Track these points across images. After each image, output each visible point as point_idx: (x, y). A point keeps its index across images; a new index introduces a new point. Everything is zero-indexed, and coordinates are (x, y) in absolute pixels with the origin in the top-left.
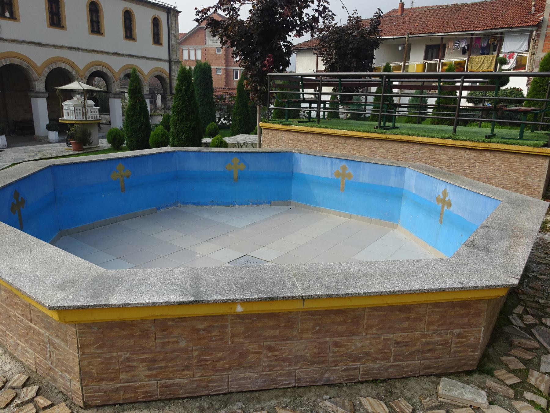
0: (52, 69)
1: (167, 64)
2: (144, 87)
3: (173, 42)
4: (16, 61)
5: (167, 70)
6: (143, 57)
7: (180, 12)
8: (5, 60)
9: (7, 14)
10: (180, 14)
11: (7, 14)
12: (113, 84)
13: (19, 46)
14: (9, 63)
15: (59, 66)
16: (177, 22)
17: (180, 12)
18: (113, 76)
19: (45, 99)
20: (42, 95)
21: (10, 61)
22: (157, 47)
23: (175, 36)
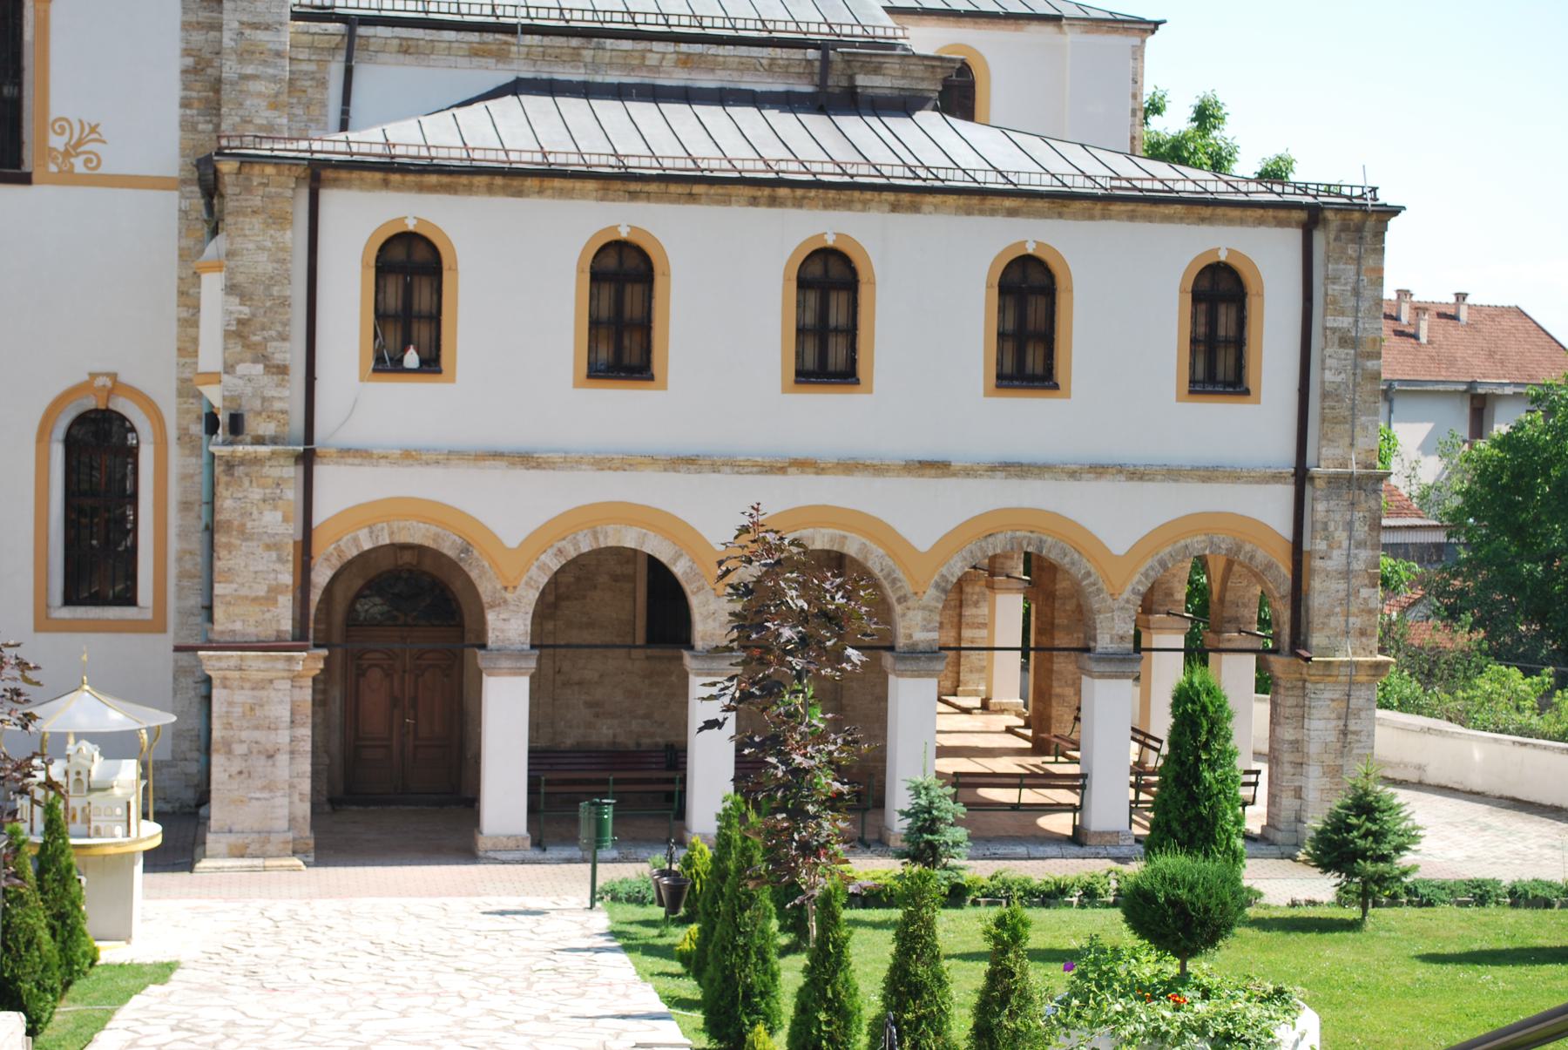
0: (573, 554)
1: (1286, 492)
2: (1100, 618)
3: (1328, 376)
4: (416, 533)
5: (1286, 530)
6: (1098, 470)
7: (1395, 211)
8: (371, 532)
9: (411, 359)
10: (1393, 223)
11: (411, 359)
12: (898, 609)
13: (437, 473)
14: (387, 541)
15: (612, 542)
16: (1370, 262)
17: (1395, 211)
18: (899, 574)
19: (522, 685)
20: (505, 664)
21: (392, 533)
22: (1219, 412)
23: (1346, 341)
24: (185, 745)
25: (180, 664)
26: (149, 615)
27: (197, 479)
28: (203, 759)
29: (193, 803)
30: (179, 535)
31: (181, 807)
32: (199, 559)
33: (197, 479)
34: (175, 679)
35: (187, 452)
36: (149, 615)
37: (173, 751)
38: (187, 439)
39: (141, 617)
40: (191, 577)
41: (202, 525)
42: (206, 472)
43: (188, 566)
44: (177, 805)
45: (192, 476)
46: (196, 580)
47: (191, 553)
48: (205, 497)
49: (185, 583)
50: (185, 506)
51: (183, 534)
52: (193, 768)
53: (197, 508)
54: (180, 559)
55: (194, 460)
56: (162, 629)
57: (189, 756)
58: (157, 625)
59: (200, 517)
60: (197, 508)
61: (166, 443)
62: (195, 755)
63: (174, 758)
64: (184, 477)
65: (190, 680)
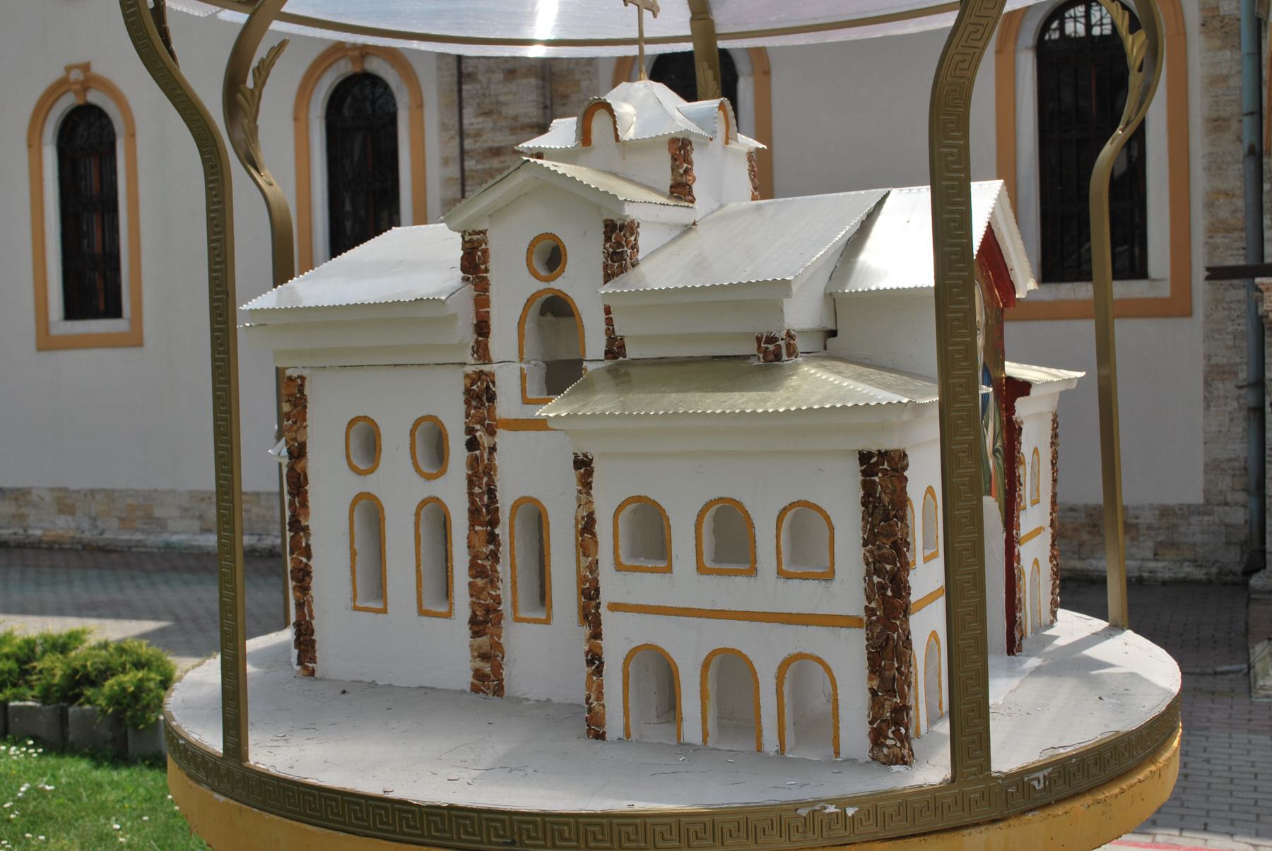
24: (1225, 482)
25: (1214, 361)
26: (1165, 291)
27: (1233, 82)
28: (1253, 503)
29: (1239, 569)
30: (1208, 169)
31: (1220, 573)
32: (1240, 203)
33: (1233, 82)
34: (1207, 383)
35: (1218, 43)
36: (1165, 291)
37: (1205, 491)
38: (1216, 24)
39: (1153, 294)
40: (1228, 230)
41: (1243, 149)
42: (1248, 67)
43: (1224, 213)
44: (1214, 570)
45: (1225, 79)
46: (1236, 235)
47: (1227, 194)
48: (1248, 104)
49: (1219, 239)
50: (1217, 124)
51: (1215, 166)
52: (1238, 516)
53: (1234, 124)
54: (1210, 205)
55: (1228, 54)
56: (1187, 312)
57: (1229, 498)
58: (1178, 306)
59: (1239, 139)
60: (1234, 124)
61: (1185, 33)
62: (1241, 497)
63: (1208, 502)
64: (1214, 81)
65: (1230, 385)
